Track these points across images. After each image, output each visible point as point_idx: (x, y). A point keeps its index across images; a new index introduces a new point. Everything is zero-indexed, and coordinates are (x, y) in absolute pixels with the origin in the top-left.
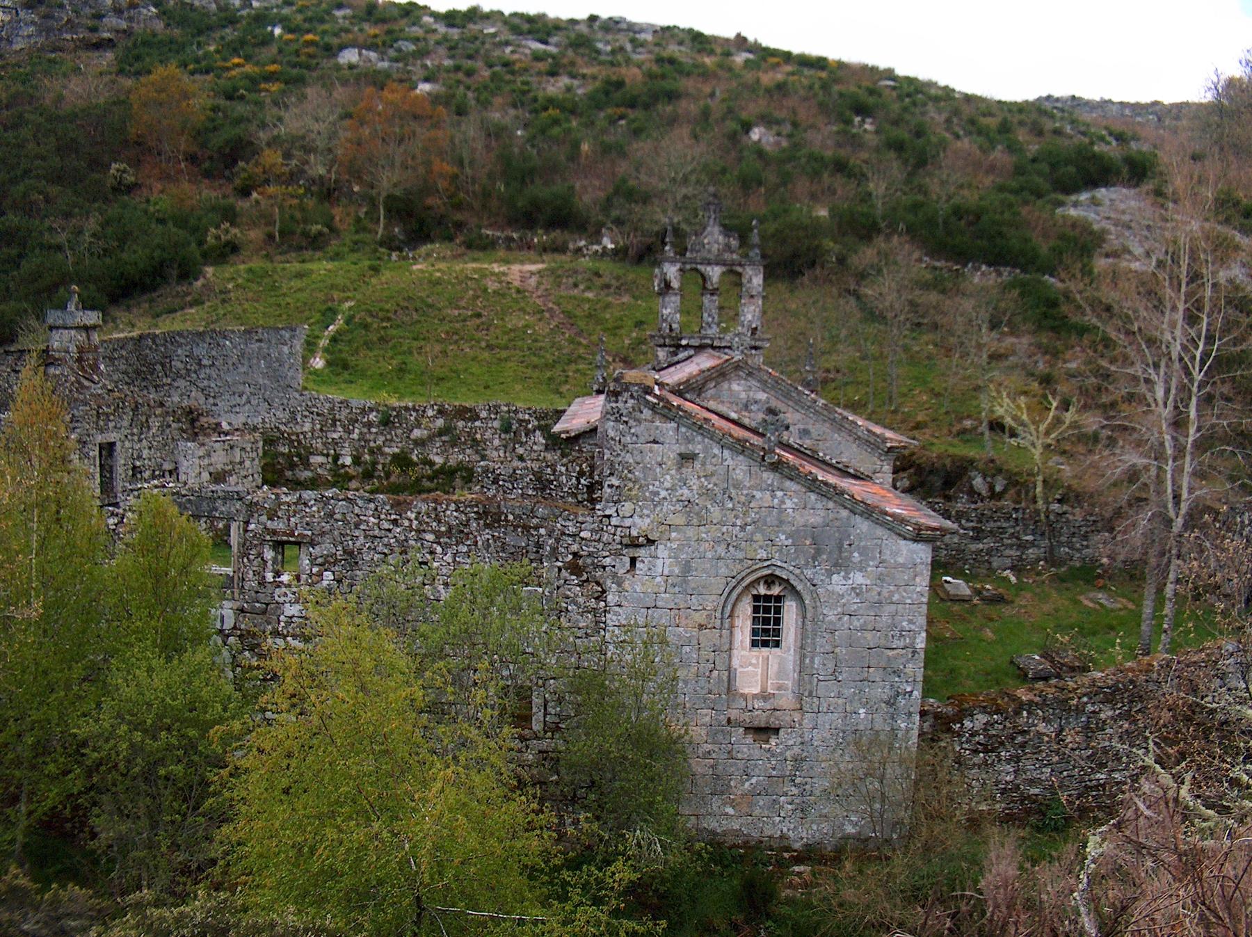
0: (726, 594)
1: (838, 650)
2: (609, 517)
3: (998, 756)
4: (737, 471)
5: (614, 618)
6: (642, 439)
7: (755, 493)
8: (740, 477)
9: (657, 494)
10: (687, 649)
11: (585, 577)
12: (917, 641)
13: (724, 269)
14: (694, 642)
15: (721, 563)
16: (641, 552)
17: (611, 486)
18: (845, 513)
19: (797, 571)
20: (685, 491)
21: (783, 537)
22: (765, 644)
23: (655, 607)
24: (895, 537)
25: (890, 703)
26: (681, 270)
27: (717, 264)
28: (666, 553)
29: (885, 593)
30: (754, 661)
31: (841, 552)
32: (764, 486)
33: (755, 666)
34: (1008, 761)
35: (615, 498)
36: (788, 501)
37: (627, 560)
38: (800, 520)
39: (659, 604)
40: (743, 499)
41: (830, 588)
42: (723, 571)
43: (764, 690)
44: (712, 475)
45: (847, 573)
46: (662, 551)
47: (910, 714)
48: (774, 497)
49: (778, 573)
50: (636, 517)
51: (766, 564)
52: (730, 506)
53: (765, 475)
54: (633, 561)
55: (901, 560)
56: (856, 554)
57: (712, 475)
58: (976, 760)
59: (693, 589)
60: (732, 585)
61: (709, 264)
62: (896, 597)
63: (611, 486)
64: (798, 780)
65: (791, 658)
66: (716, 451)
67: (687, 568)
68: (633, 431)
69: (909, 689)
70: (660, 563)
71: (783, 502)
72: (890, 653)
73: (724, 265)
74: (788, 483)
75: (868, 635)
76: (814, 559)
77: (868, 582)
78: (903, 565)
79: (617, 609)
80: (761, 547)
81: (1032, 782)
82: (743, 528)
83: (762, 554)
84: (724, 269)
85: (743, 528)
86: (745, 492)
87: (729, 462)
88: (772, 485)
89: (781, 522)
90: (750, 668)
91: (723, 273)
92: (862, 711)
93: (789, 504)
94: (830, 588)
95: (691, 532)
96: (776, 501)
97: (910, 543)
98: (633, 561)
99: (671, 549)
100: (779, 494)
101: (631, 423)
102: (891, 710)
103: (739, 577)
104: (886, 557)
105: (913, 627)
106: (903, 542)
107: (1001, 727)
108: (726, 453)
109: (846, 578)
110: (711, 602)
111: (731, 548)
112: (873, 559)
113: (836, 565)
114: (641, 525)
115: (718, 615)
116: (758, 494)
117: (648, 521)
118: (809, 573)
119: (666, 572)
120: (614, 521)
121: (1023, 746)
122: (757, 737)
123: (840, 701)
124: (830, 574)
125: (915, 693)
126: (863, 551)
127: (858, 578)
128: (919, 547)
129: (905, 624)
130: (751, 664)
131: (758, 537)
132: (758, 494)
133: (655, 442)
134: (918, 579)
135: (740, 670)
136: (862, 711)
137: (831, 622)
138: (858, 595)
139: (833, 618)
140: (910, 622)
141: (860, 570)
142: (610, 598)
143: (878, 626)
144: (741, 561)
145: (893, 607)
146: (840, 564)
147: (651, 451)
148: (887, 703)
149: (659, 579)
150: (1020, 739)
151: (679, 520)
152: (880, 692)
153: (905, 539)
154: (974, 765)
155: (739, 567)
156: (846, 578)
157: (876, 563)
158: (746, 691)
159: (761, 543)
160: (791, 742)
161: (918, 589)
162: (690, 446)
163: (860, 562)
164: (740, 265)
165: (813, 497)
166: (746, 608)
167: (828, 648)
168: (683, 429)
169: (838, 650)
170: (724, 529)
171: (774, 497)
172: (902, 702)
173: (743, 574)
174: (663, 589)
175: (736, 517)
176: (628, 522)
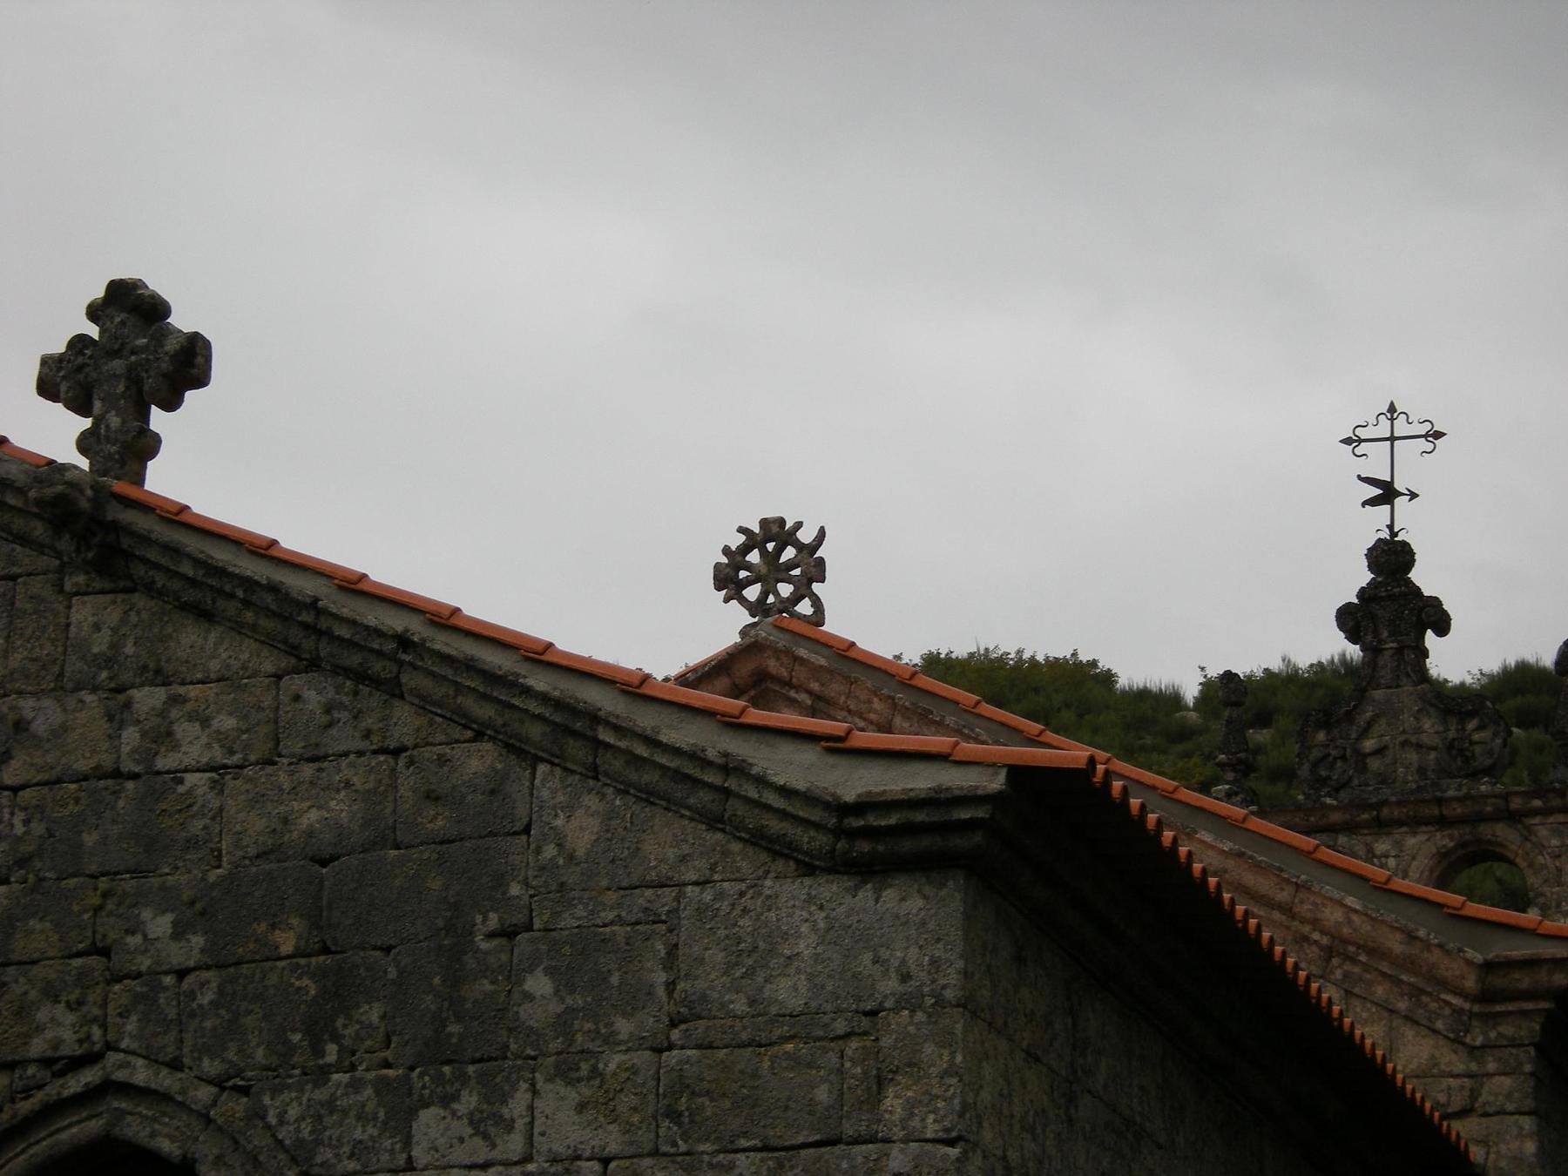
7: (27, 706)
13: (1444, 840)
18: (478, 761)
21: (160, 925)
24: (746, 861)
27: (1415, 823)
32: (74, 665)
36: (186, 730)
45: (496, 1095)
48: (118, 716)
51: (75, 1084)
53: (82, 614)
55: (788, 992)
56: (539, 984)
61: (1381, 826)
71: (163, 737)
73: (1442, 822)
74: (191, 642)
76: (318, 1030)
77: (613, 1140)
80: (51, 993)
83: (60, 1029)
84: (1444, 840)
88: (110, 660)
91: (1443, 855)
93: (193, 745)
97: (829, 888)
100: (147, 699)
106: (793, 890)
109: (486, 1124)
116: (43, 714)
128: (902, 902)
132: (43, 714)
134: (893, 1103)
141: (565, 1073)
153: (807, 869)
156: (486, 1124)
157: (649, 1021)
163: (563, 1024)
164: (1513, 818)
165: (314, 694)
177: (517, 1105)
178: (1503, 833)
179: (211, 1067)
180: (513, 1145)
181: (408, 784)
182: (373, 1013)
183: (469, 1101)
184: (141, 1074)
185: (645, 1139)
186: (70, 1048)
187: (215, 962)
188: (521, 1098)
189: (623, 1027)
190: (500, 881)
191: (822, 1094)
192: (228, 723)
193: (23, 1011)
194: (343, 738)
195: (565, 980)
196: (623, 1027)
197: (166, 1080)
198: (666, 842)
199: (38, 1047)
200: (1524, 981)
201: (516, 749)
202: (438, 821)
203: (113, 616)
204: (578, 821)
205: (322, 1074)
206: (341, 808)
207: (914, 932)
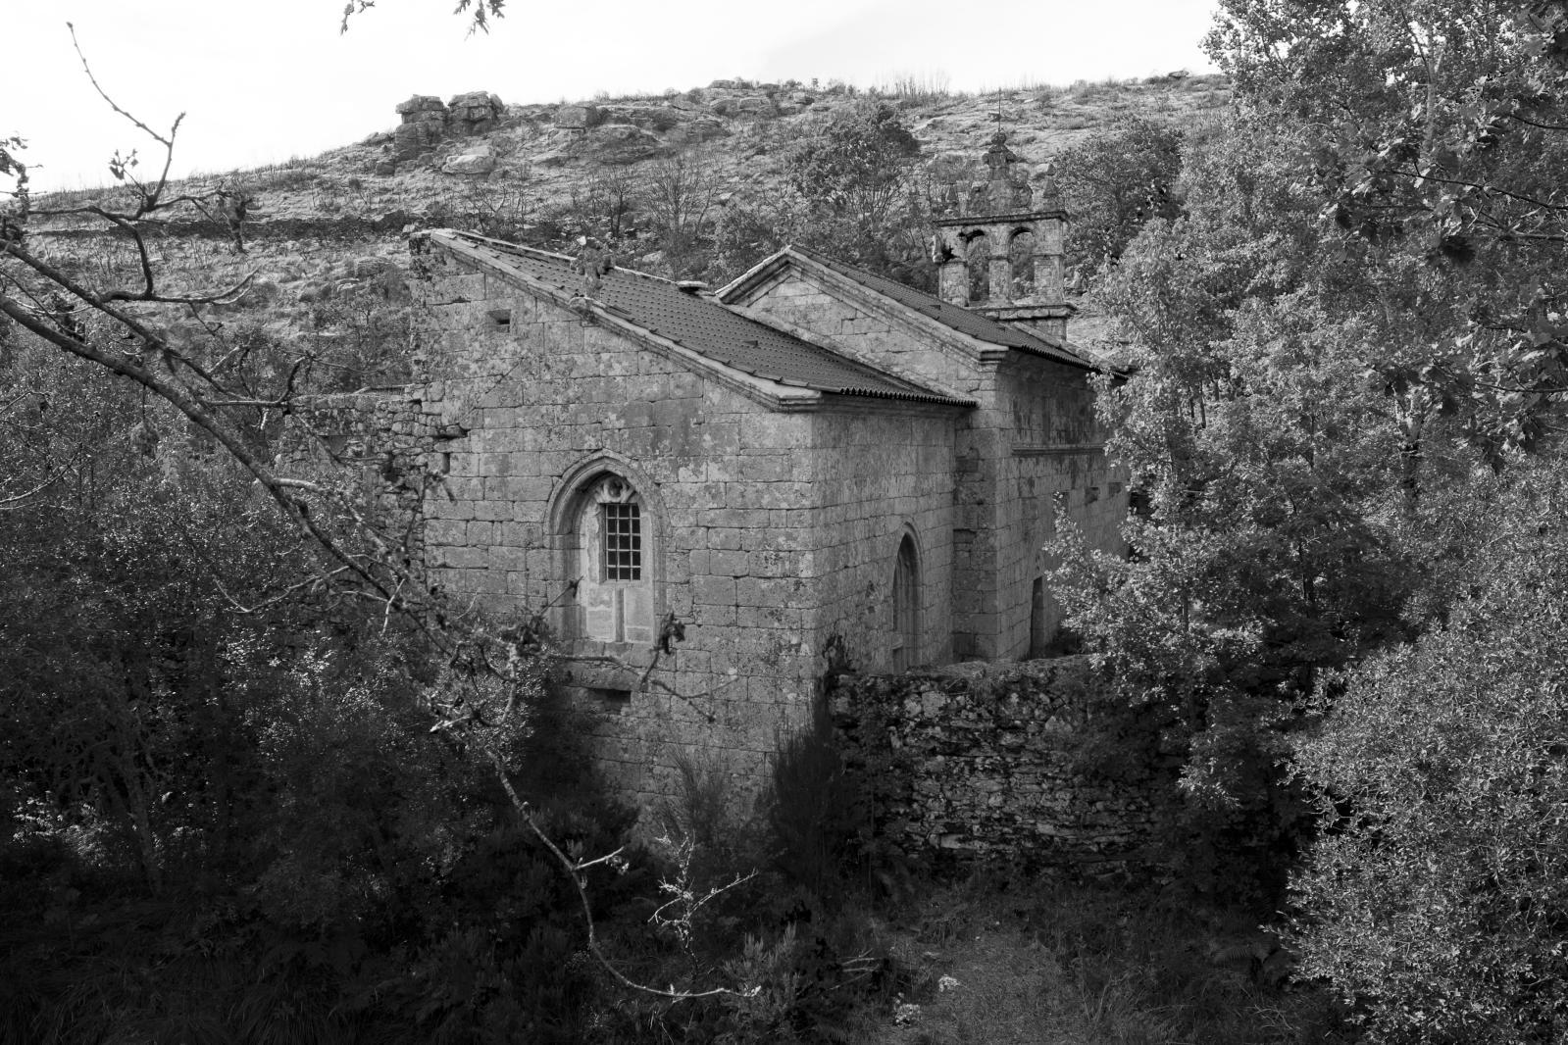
0: (552, 500)
1: (695, 578)
2: (418, 402)
3: (971, 764)
4: (554, 330)
5: (432, 534)
6: (447, 299)
8: (558, 338)
9: (466, 368)
10: (512, 576)
11: (400, 482)
12: (801, 566)
14: (521, 567)
15: (543, 457)
16: (454, 446)
17: (417, 362)
18: (689, 378)
19: (635, 465)
20: (498, 362)
21: (613, 417)
22: (625, 574)
23: (474, 519)
24: (758, 408)
25: (771, 661)
26: (961, 235)
28: (481, 445)
29: (751, 495)
30: (606, 597)
31: (686, 435)
33: (608, 604)
34: (990, 772)
35: (423, 377)
36: (616, 365)
37: (439, 457)
38: (633, 392)
39: (478, 514)
40: (562, 366)
41: (676, 487)
42: (547, 468)
43: (620, 636)
44: (526, 336)
45: (698, 465)
46: (475, 442)
47: (799, 680)
48: (598, 361)
49: (611, 468)
50: (445, 400)
52: (548, 377)
53: (587, 332)
54: (447, 455)
55: (769, 443)
56: (707, 437)
57: (526, 336)
58: (930, 765)
59: (515, 493)
60: (559, 486)
61: (994, 223)
62: (766, 500)
63: (417, 362)
64: (657, 770)
65: (650, 593)
66: (529, 305)
67: (505, 467)
68: (437, 288)
69: (794, 641)
70: (474, 459)
72: (764, 585)
73: (1012, 222)
75: (734, 557)
76: (654, 446)
78: (772, 451)
79: (433, 522)
80: (588, 433)
81: (1036, 812)
82: (565, 406)
83: (591, 442)
85: (565, 406)
86: (564, 357)
87: (544, 318)
89: (609, 396)
90: (602, 607)
92: (732, 671)
93: (617, 370)
94: (676, 487)
95: (505, 416)
96: (602, 366)
97: (779, 416)
98: (447, 455)
99: (484, 439)
100: (605, 356)
101: (436, 278)
102: (772, 672)
103: (566, 476)
104: (749, 439)
105: (794, 545)
107: (972, 716)
108: (541, 305)
110: (536, 513)
111: (553, 436)
112: (730, 443)
113: (682, 453)
114: (449, 411)
115: (546, 529)
116: (579, 359)
117: (458, 404)
118: (648, 466)
119: (483, 473)
120: (425, 407)
121: (1017, 750)
122: (609, 704)
123: (703, 655)
124: (676, 468)
125: (805, 647)
126: (716, 431)
127: (713, 472)
128: (798, 420)
129: (781, 540)
130: (602, 602)
131: (583, 418)
133: (461, 300)
134: (795, 471)
135: (590, 609)
136: (732, 671)
137: (682, 539)
138: (714, 497)
139: (683, 532)
140: (789, 537)
141: (714, 460)
142: (425, 507)
143: (746, 544)
144: (567, 452)
145: (763, 515)
146: (688, 454)
147: (457, 313)
148: (766, 660)
149: (475, 482)
150: (1008, 739)
151: (492, 400)
152: (755, 643)
153: (773, 411)
154: (929, 773)
155: (565, 462)
156: (696, 472)
158: (598, 639)
159: (587, 427)
160: (643, 713)
161: (797, 486)
162: (499, 301)
163: (714, 448)
165: (647, 357)
166: (591, 522)
167: (681, 576)
168: (490, 280)
169: (695, 578)
170: (543, 410)
171: (598, 361)
172: (786, 659)
173: (571, 471)
174: (480, 494)
175: (556, 392)
176: (437, 408)
177: (703, 468)
178: (1031, 226)
179: (629, 454)
180: (703, 478)
181: (672, 383)
182: (667, 442)
183: (692, 466)
184: (612, 455)
185: (735, 478)
186: (594, 447)
187: (627, 427)
188: (704, 467)
189: (728, 449)
190: (696, 410)
191: (778, 469)
192: (625, 364)
193: (582, 437)
194: (655, 369)
195: (714, 438)
196: (728, 449)
197: (618, 456)
198: (737, 402)
199: (586, 447)
200: (992, 356)
201: (699, 375)
202: (679, 393)
203: (595, 333)
204: (715, 395)
205: (655, 458)
206: (655, 388)
207: (800, 428)
